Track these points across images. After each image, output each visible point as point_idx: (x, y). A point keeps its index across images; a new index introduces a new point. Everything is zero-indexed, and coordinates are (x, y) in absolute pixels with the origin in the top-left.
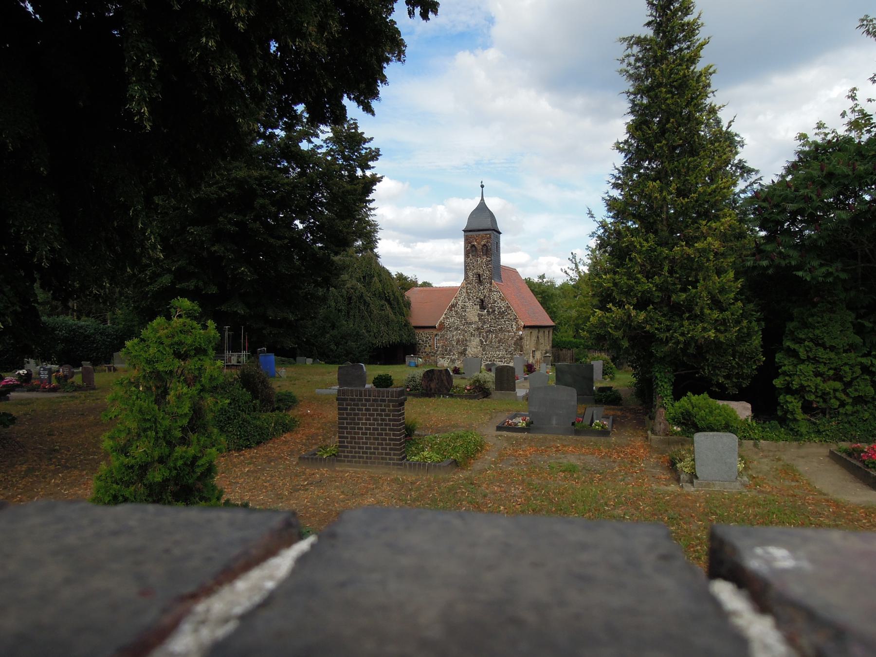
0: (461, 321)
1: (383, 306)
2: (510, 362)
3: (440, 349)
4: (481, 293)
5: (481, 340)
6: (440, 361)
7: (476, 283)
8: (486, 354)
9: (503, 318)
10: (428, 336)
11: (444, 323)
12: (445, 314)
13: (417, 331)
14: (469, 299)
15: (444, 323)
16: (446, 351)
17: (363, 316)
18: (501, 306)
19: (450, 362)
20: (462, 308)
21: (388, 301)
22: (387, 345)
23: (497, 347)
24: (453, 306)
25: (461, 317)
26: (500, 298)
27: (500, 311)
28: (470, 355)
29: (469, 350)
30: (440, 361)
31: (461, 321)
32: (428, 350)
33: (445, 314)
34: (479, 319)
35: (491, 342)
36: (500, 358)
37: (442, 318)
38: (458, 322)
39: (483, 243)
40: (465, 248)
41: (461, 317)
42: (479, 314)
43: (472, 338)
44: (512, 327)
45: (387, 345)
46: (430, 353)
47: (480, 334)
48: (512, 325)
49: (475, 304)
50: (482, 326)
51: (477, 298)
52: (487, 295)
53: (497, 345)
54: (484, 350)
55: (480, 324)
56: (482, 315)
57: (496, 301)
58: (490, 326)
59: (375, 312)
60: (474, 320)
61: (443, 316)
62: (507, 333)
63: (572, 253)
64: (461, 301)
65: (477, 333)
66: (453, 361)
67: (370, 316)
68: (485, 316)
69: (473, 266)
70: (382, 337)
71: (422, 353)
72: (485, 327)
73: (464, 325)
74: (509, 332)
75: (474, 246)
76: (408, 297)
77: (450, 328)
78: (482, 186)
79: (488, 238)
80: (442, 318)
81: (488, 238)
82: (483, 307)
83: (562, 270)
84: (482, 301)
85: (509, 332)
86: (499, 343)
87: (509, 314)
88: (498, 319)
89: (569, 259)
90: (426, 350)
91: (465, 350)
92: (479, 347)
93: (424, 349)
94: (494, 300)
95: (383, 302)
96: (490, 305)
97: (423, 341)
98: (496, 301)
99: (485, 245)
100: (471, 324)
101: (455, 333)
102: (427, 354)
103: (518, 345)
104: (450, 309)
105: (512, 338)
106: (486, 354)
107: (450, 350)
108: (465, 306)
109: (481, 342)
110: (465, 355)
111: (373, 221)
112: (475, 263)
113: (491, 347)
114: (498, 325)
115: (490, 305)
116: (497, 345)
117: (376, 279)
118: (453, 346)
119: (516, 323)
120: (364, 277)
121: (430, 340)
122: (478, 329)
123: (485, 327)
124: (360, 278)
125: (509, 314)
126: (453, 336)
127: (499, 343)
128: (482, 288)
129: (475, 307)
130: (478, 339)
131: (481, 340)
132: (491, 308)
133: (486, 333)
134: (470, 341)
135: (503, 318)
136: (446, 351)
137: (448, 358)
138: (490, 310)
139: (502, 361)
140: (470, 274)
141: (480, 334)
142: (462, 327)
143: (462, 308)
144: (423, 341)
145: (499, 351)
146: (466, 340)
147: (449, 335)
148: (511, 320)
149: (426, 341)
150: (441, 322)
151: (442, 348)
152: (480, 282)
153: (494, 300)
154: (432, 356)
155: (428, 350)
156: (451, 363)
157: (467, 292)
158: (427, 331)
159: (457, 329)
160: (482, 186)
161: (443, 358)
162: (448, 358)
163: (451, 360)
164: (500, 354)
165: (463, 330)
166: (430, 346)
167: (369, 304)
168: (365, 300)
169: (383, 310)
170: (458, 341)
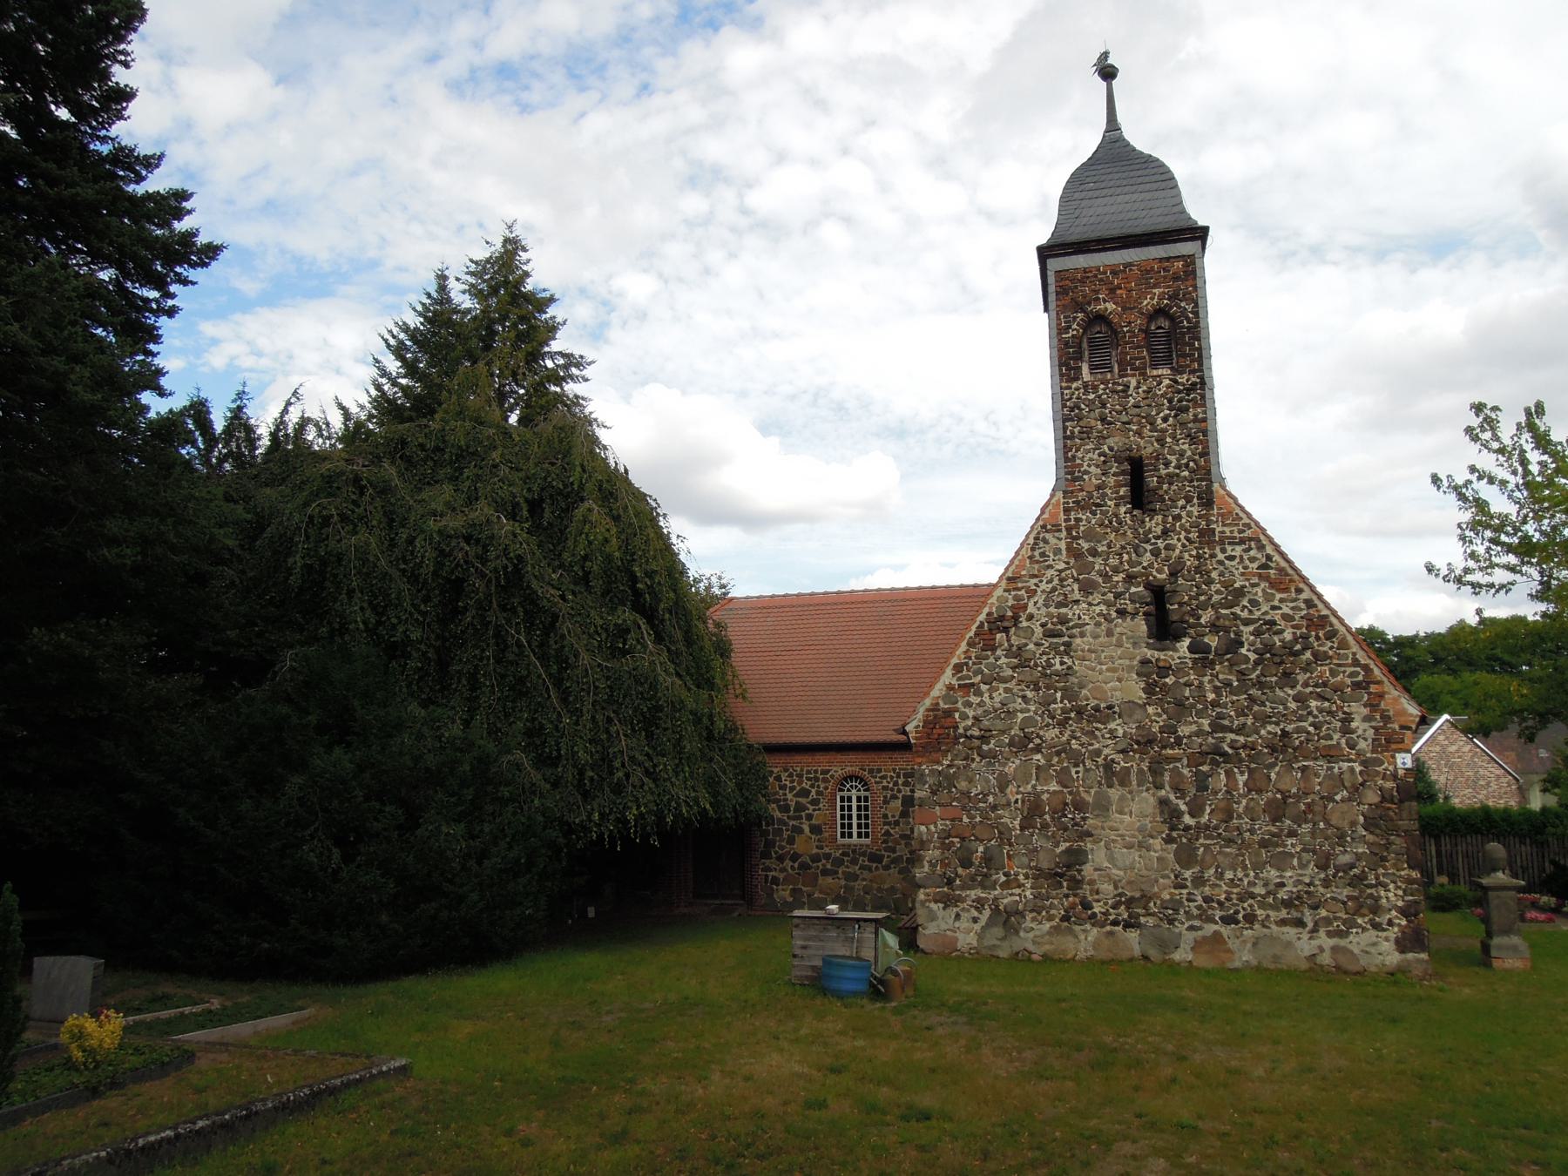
0: (1046, 703)
1: (623, 632)
2: (1351, 924)
3: (932, 854)
4: (1156, 553)
5: (1163, 802)
6: (932, 917)
7: (1119, 501)
8: (1199, 881)
9: (1287, 678)
10: (806, 785)
11: (949, 713)
12: (958, 668)
13: (775, 764)
14: (1087, 588)
15: (949, 713)
16: (967, 863)
17: (522, 680)
18: (1276, 616)
19: (991, 923)
20: (1050, 634)
21: (650, 615)
22: (645, 837)
23: (1264, 844)
24: (999, 623)
25: (1045, 681)
26: (1267, 578)
27: (1268, 647)
28: (1107, 888)
29: (1097, 856)
30: (932, 917)
31: (1046, 703)
32: (805, 845)
33: (958, 668)
34: (1149, 690)
35: (1229, 815)
36: (1287, 904)
37: (938, 690)
38: (1026, 710)
39: (1148, 303)
40: (1058, 331)
41: (1045, 681)
42: (1145, 662)
43: (1114, 793)
44: (1346, 730)
45: (645, 837)
46: (816, 859)
47: (1156, 769)
48: (1348, 719)
49: (1122, 613)
50: (1170, 729)
51: (1130, 579)
52: (1190, 562)
53: (1264, 827)
54: (1186, 857)
55: (1155, 717)
56: (1164, 670)
57: (1240, 593)
58: (1216, 727)
59: (585, 658)
60: (1117, 697)
61: (948, 677)
62: (1321, 766)
63: (1478, 408)
64: (1041, 600)
65: (1136, 764)
66: (1007, 919)
67: (558, 682)
68: (1179, 671)
69: (1103, 420)
70: (618, 789)
71: (781, 859)
72: (1184, 730)
73: (1063, 724)
74: (1331, 755)
75: (1101, 318)
76: (717, 625)
77: (984, 739)
78: (1107, 73)
79: (1176, 278)
80: (938, 690)
81: (1176, 278)
82: (1164, 629)
83: (1436, 480)
84: (1159, 595)
85: (1331, 755)
86: (1275, 819)
87: (1319, 657)
88: (1260, 685)
89: (1469, 430)
90: (799, 846)
91: (1076, 858)
92: (1157, 843)
93: (791, 841)
94: (1227, 585)
95: (626, 615)
96: (1206, 617)
97: (785, 809)
98: (1240, 593)
99: (1160, 312)
100: (1103, 714)
101: (1010, 768)
102: (804, 866)
103: (1396, 830)
104: (985, 640)
105: (1356, 790)
106: (1199, 881)
107: (988, 859)
108: (1063, 620)
109: (1170, 815)
110: (1076, 884)
111: (577, 397)
112: (1113, 403)
113: (1230, 842)
114: (1264, 719)
115: (1206, 617)
116: (1264, 827)
117: (591, 506)
118: (1004, 835)
119: (1373, 706)
120: (535, 506)
121: (815, 802)
122: (1145, 742)
123: (1184, 730)
124: (516, 505)
125: (1319, 657)
126: (1003, 784)
127: (1274, 820)
128: (1154, 524)
129: (1122, 626)
130: (1145, 801)
131: (1163, 802)
132: (1215, 627)
133: (1194, 761)
134: (1103, 807)
135: (1287, 678)
136: (967, 863)
137: (979, 904)
138: (1213, 641)
139: (1299, 923)
140: (1089, 458)
141: (1156, 769)
142: (1051, 734)
143: (1050, 634)
144: (785, 809)
145: (1281, 862)
146: (1080, 806)
147: (981, 778)
148: (1337, 689)
149: (800, 808)
150: (934, 708)
151: (945, 847)
152: (1140, 497)
153: (1227, 585)
154: (825, 872)
155: (805, 845)
156: (998, 931)
157: (1075, 553)
158: (801, 763)
159: (1022, 744)
160: (1107, 73)
161: (948, 901)
162: (979, 904)
163: (996, 911)
164: (1291, 879)
165: (1063, 750)
166: (816, 830)
167: (555, 617)
168: (531, 600)
169: (624, 652)
170: (1032, 811)
